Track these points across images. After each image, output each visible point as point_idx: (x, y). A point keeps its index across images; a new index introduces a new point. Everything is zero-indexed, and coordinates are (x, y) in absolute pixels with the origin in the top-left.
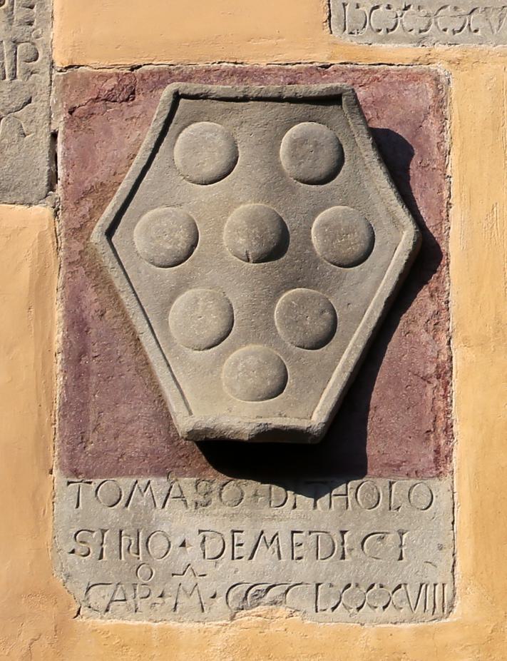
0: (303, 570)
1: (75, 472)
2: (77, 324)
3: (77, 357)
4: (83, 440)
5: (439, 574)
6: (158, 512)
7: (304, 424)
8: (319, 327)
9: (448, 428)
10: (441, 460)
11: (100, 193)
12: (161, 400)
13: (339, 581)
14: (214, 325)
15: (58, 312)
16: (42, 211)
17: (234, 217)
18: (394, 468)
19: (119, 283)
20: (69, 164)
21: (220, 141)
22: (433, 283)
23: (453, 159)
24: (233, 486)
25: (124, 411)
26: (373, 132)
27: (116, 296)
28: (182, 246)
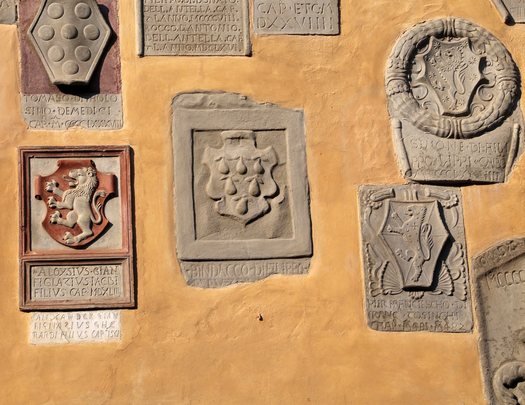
0: (85, 117)
1: (26, 92)
2: (25, 55)
3: (25, 63)
4: (27, 85)
5: (119, 118)
6: (47, 103)
7: (83, 80)
8: (86, 56)
9: (120, 81)
10: (119, 89)
11: (29, 21)
12: (47, 75)
13: (94, 120)
14: (60, 55)
15: (19, 52)
16: (14, 26)
17: (63, 28)
18: (107, 91)
19: (35, 45)
20: (20, 14)
21: (59, 8)
22: (115, 44)
23: (119, 12)
24: (66, 96)
25: (37, 77)
26: (99, 5)
27: (34, 48)
28: (51, 35)
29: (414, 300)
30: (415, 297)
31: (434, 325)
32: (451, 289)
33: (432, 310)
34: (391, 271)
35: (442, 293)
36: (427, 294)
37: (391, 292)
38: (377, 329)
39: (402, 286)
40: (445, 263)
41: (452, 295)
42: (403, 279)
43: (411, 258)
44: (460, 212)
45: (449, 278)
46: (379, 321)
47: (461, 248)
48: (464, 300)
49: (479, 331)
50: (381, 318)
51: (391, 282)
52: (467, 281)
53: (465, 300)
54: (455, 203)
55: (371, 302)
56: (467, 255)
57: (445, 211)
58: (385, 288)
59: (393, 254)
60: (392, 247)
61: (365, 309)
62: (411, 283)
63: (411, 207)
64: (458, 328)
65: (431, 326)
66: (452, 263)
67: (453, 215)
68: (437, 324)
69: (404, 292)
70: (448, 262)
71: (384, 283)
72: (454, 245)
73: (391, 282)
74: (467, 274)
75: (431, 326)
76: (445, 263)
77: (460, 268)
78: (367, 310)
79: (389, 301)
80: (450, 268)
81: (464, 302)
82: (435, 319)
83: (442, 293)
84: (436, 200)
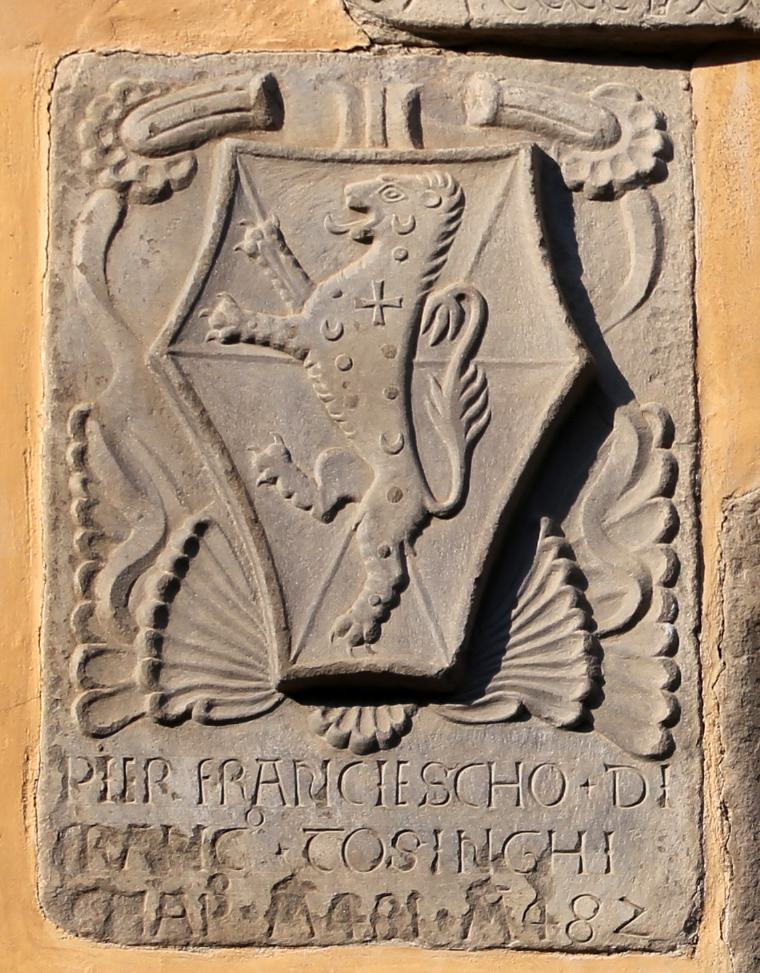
29: (346, 756)
30: (356, 738)
31: (458, 907)
32: (581, 689)
33: (452, 817)
34: (219, 580)
35: (523, 714)
36: (429, 718)
37: (210, 706)
38: (103, 934)
39: (275, 675)
40: (555, 530)
41: (583, 724)
42: (286, 629)
43: (344, 501)
44: (675, 219)
45: (577, 622)
46: (119, 883)
47: (667, 440)
48: (654, 758)
49: (734, 944)
50: (135, 864)
51: (215, 646)
52: (686, 643)
53: (665, 754)
54: (648, 164)
55: (76, 769)
56: (696, 485)
57: (585, 211)
58: (173, 682)
59: (235, 474)
60: (229, 436)
61: (38, 809)
62: (328, 653)
63: (367, 192)
64: (602, 929)
65: (443, 914)
66: (601, 531)
67: (631, 236)
68: (481, 901)
69: (291, 708)
70: (577, 525)
71: (170, 655)
72: (621, 419)
73: (215, 646)
74: (687, 600)
75: (443, 914)
76: (555, 530)
77: (650, 563)
78: (51, 818)
79: (190, 762)
80: (588, 561)
81: (656, 767)
82: (469, 873)
83: (523, 714)
84: (522, 147)
